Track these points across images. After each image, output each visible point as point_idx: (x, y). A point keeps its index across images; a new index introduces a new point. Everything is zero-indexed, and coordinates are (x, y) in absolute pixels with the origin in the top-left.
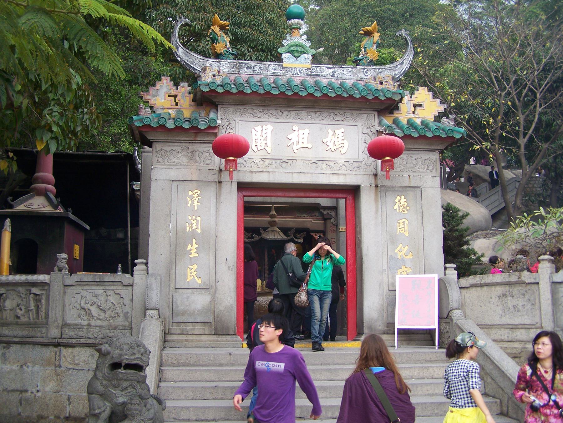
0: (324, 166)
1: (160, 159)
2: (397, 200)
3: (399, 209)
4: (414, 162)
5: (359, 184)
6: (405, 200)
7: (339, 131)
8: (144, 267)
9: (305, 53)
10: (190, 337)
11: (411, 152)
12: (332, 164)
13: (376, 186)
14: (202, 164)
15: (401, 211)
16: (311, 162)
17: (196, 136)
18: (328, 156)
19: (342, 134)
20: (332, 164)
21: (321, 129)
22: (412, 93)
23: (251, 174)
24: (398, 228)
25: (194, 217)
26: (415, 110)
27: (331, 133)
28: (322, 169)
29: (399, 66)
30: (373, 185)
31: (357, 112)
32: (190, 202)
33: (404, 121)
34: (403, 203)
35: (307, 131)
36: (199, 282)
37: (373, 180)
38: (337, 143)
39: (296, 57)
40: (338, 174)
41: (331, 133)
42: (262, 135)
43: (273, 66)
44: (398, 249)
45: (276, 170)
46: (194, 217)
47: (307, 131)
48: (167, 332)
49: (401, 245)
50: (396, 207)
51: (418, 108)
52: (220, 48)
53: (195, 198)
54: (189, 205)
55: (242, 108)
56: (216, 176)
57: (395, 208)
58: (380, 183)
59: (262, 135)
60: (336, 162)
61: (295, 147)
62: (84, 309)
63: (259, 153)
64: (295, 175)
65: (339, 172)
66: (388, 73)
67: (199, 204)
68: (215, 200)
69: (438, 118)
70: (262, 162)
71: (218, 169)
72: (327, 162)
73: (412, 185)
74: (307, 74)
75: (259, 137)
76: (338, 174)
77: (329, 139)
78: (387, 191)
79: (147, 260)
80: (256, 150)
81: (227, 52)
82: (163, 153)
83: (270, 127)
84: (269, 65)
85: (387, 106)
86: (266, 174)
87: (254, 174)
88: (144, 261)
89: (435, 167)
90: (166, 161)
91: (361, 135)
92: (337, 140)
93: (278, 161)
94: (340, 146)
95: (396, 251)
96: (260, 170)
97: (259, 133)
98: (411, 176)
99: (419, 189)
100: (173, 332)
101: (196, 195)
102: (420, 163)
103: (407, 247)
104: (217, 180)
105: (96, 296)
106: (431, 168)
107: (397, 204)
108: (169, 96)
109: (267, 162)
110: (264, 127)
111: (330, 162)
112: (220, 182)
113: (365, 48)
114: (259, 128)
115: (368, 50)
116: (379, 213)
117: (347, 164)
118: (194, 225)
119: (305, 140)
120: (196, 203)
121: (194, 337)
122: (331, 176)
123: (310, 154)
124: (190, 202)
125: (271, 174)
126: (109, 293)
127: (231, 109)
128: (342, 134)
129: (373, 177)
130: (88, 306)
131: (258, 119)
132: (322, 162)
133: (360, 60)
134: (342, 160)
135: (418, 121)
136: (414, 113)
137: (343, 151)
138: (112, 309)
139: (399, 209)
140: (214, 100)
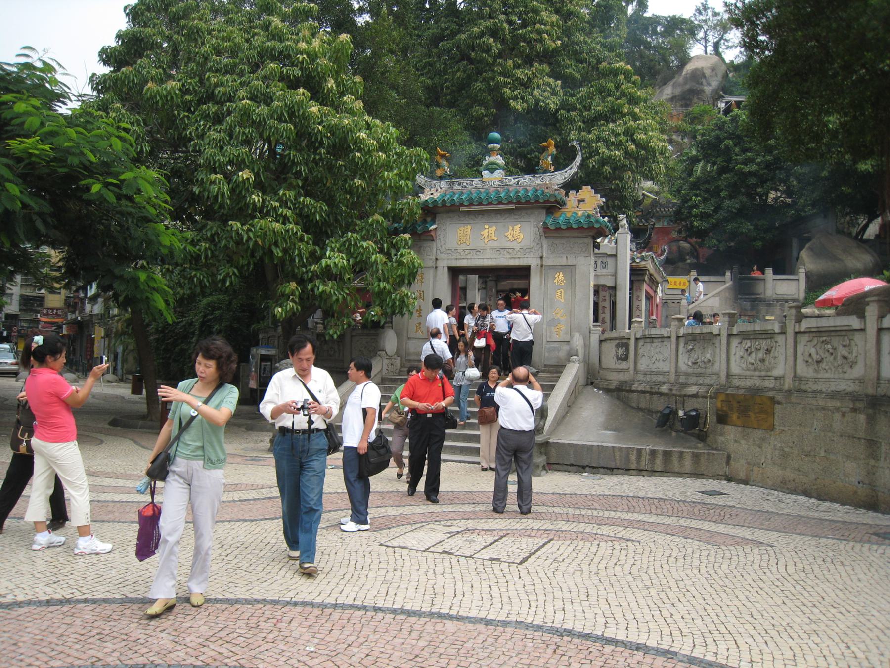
7: (517, 227)
13: (542, 266)
18: (509, 245)
22: (578, 192)
27: (511, 228)
35: (494, 228)
41: (511, 228)
43: (476, 181)
47: (494, 228)
55: (451, 215)
58: (544, 263)
60: (513, 249)
66: (561, 177)
73: (569, 263)
83: (469, 227)
85: (552, 206)
114: (462, 228)
123: (495, 245)
134: (517, 247)
137: (519, 240)
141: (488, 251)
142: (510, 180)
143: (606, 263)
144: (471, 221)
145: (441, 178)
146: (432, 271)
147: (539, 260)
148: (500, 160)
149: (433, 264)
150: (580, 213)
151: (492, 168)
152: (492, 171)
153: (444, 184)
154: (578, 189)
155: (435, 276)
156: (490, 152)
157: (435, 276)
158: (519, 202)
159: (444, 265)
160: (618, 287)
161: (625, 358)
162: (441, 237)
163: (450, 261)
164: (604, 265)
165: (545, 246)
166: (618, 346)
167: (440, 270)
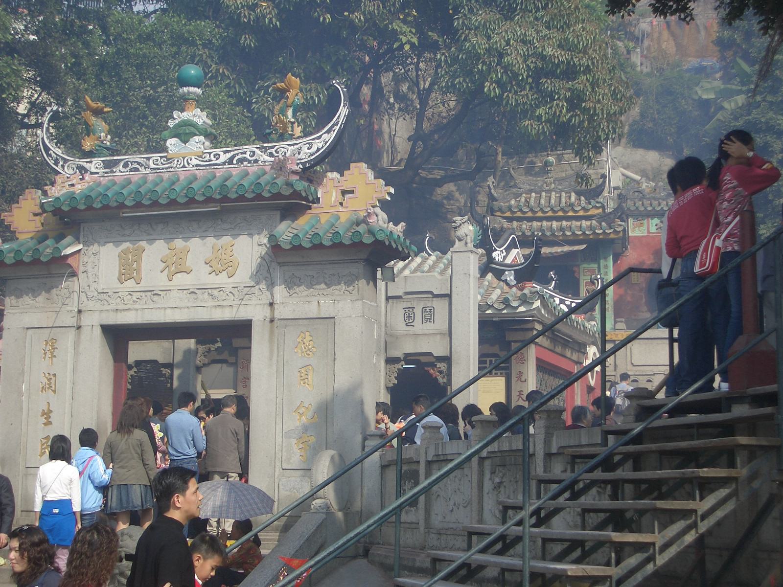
0: (206, 296)
6: (310, 338)
12: (215, 292)
13: (272, 321)
16: (189, 292)
20: (215, 292)
30: (268, 319)
37: (269, 311)
39: (185, 142)
51: (347, 196)
56: (75, 319)
58: (277, 315)
60: (220, 289)
64: (169, 311)
65: (225, 303)
70: (129, 297)
71: (76, 310)
74: (197, 165)
84: (148, 159)
86: (134, 312)
87: (119, 313)
93: (149, 293)
98: (322, 302)
99: (332, 320)
111: (213, 290)
112: (79, 328)
116: (275, 358)
117: (235, 291)
122: (213, 309)
125: (139, 311)
132: (203, 291)
136: (341, 204)
141: (174, 294)
142: (217, 156)
143: (432, 310)
145: (90, 154)
147: (267, 309)
148: (198, 116)
149: (72, 321)
150: (344, 218)
151: (185, 132)
153: (95, 165)
154: (342, 168)
157: (77, 343)
158: (225, 199)
159: (93, 321)
160: (454, 358)
162: (89, 268)
163: (104, 315)
164: (428, 315)
167: (85, 331)
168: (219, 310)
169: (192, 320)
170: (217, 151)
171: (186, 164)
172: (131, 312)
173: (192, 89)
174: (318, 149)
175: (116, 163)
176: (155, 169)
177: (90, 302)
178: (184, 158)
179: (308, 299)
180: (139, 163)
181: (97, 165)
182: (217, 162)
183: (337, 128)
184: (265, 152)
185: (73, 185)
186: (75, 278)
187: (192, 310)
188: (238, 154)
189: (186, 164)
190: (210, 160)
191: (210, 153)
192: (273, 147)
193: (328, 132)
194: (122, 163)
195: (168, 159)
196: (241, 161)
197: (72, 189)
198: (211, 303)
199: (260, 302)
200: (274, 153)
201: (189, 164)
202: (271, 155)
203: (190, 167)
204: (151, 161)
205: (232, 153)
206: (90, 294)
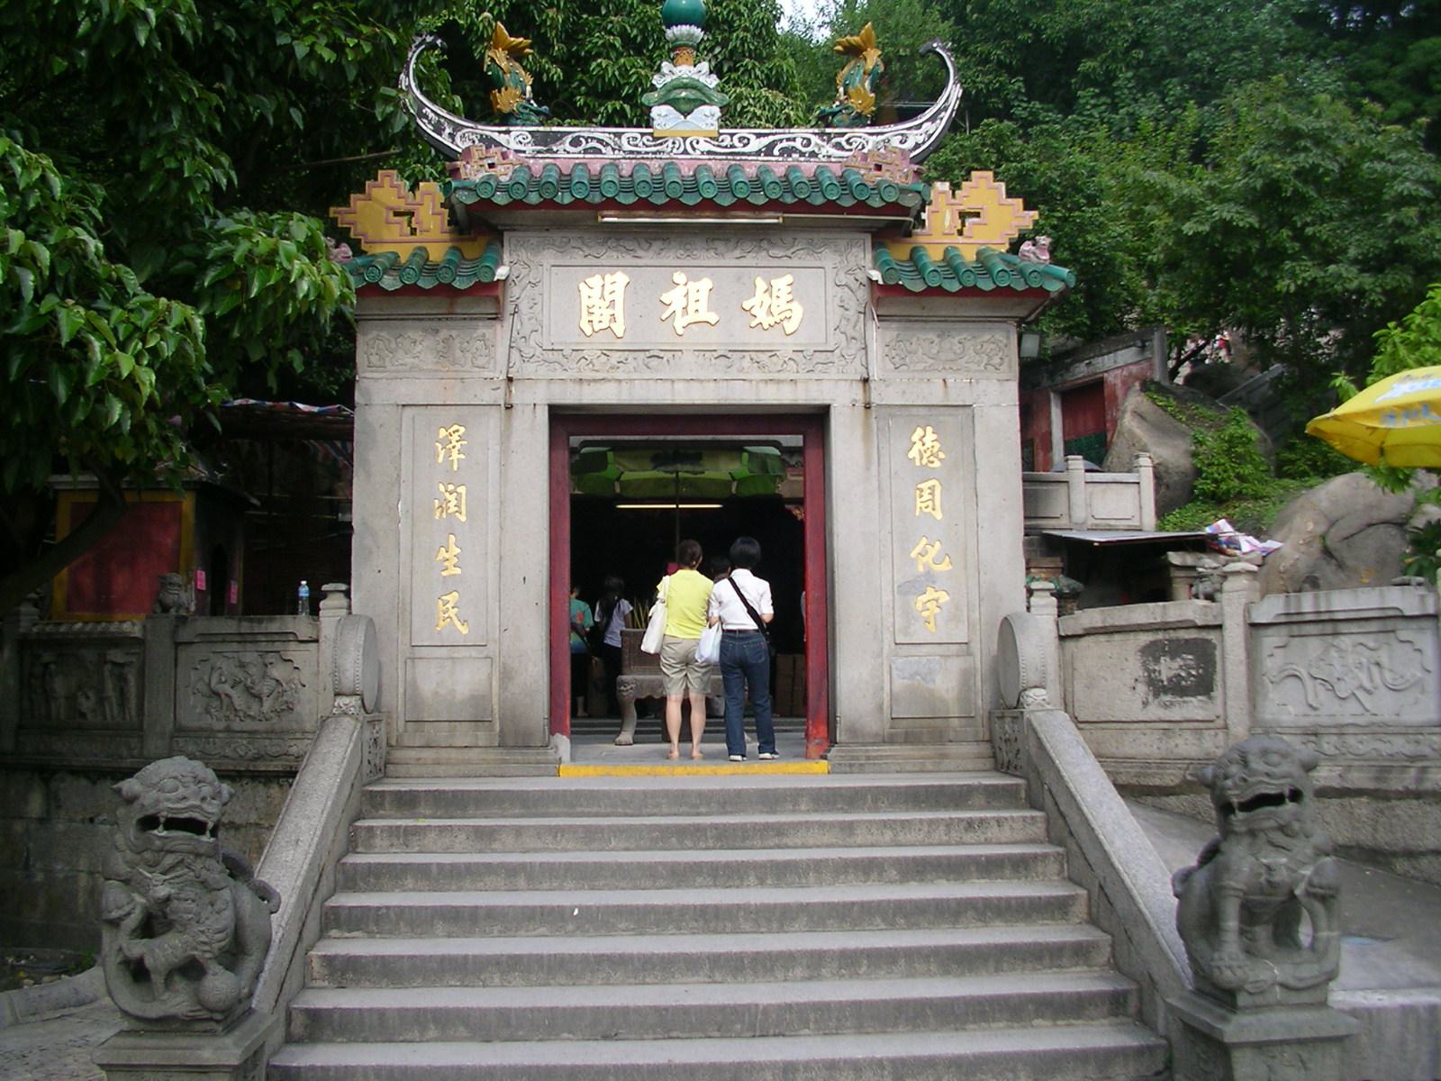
0: (746, 363)
1: (374, 359)
2: (915, 438)
3: (921, 458)
4: (957, 348)
5: (827, 402)
6: (935, 437)
7: (782, 283)
8: (344, 602)
9: (704, 103)
10: (444, 754)
11: (949, 325)
12: (764, 357)
13: (868, 407)
14: (468, 367)
15: (925, 461)
16: (716, 354)
17: (452, 305)
19: (789, 289)
21: (739, 279)
22: (955, 187)
23: (577, 386)
24: (919, 500)
25: (451, 487)
26: (963, 224)
27: (761, 284)
28: (742, 370)
29: (924, 126)
30: (860, 405)
31: (823, 235)
32: (442, 453)
33: (934, 255)
34: (929, 444)
35: (706, 284)
36: (464, 630)
37: (860, 391)
38: (775, 310)
39: (686, 114)
40: (779, 381)
42: (602, 297)
44: (918, 549)
45: (635, 376)
46: (451, 487)
48: (394, 743)
49: (924, 541)
50: (913, 453)
51: (969, 221)
52: (506, 100)
53: (454, 443)
54: (440, 460)
55: (557, 236)
56: (501, 393)
57: (911, 455)
58: (875, 399)
59: (602, 297)
60: (773, 353)
61: (680, 323)
62: (217, 694)
63: (596, 338)
64: (679, 386)
65: (782, 376)
67: (462, 456)
68: (497, 448)
69: (1015, 247)
71: (503, 377)
72: (753, 354)
74: (709, 153)
75: (596, 301)
76: (779, 381)
77: (758, 302)
78: (892, 416)
79: (349, 583)
80: (588, 331)
81: (526, 108)
82: (382, 346)
83: (621, 278)
86: (613, 385)
87: (585, 386)
88: (343, 587)
89: (1006, 360)
90: (387, 363)
91: (832, 290)
92: (775, 302)
93: (641, 355)
94: (782, 316)
95: (913, 554)
96: (599, 376)
97: (596, 293)
98: (950, 381)
99: (968, 410)
100: (407, 742)
101: (455, 437)
102: (971, 352)
103: (938, 545)
104: (502, 403)
105: (242, 665)
106: (996, 360)
107: (918, 446)
108: (397, 214)
109: (615, 357)
110: (608, 277)
111: (760, 354)
112: (509, 407)
113: (846, 86)
114: (595, 281)
115: (851, 90)
116: (874, 468)
118: (451, 505)
119: (703, 305)
120: (455, 455)
121: (453, 754)
122: (762, 385)
123: (713, 338)
124: (442, 453)
125: (624, 384)
126: (270, 658)
127: (534, 241)
128: (789, 289)
129: (861, 385)
130: (227, 688)
131: (594, 261)
133: (834, 114)
135: (969, 255)
136: (960, 233)
137: (790, 327)
138: (275, 694)
139: (921, 458)
140: (494, 222)
141: (688, 357)
144: (628, 260)
146: (494, 419)
147: (858, 388)
148: (701, 73)
149: (499, 397)
152: (685, 107)
153: (516, 138)
155: (506, 434)
156: (674, 51)
157: (506, 434)
159: (535, 398)
161: (1204, 686)
162: (524, 307)
165: (874, 347)
166: (1152, 652)
168: (771, 388)
169: (723, 402)
170: (744, 133)
171: (689, 149)
172: (608, 384)
173: (685, 29)
174: (917, 146)
175: (558, 137)
176: (632, 152)
177: (527, 364)
178: (685, 139)
179: (927, 375)
180: (600, 141)
181: (520, 138)
182: (746, 150)
183: (945, 116)
184: (828, 142)
185: (492, 166)
186: (498, 325)
187: (721, 384)
188: (781, 141)
189: (689, 149)
190: (732, 146)
191: (732, 135)
192: (843, 135)
193: (933, 119)
194: (569, 138)
195: (655, 139)
196: (787, 152)
197: (492, 171)
198: (757, 375)
199: (845, 377)
200: (844, 144)
201: (694, 149)
202: (839, 146)
203: (697, 155)
204: (624, 139)
205: (771, 138)
206: (528, 352)
